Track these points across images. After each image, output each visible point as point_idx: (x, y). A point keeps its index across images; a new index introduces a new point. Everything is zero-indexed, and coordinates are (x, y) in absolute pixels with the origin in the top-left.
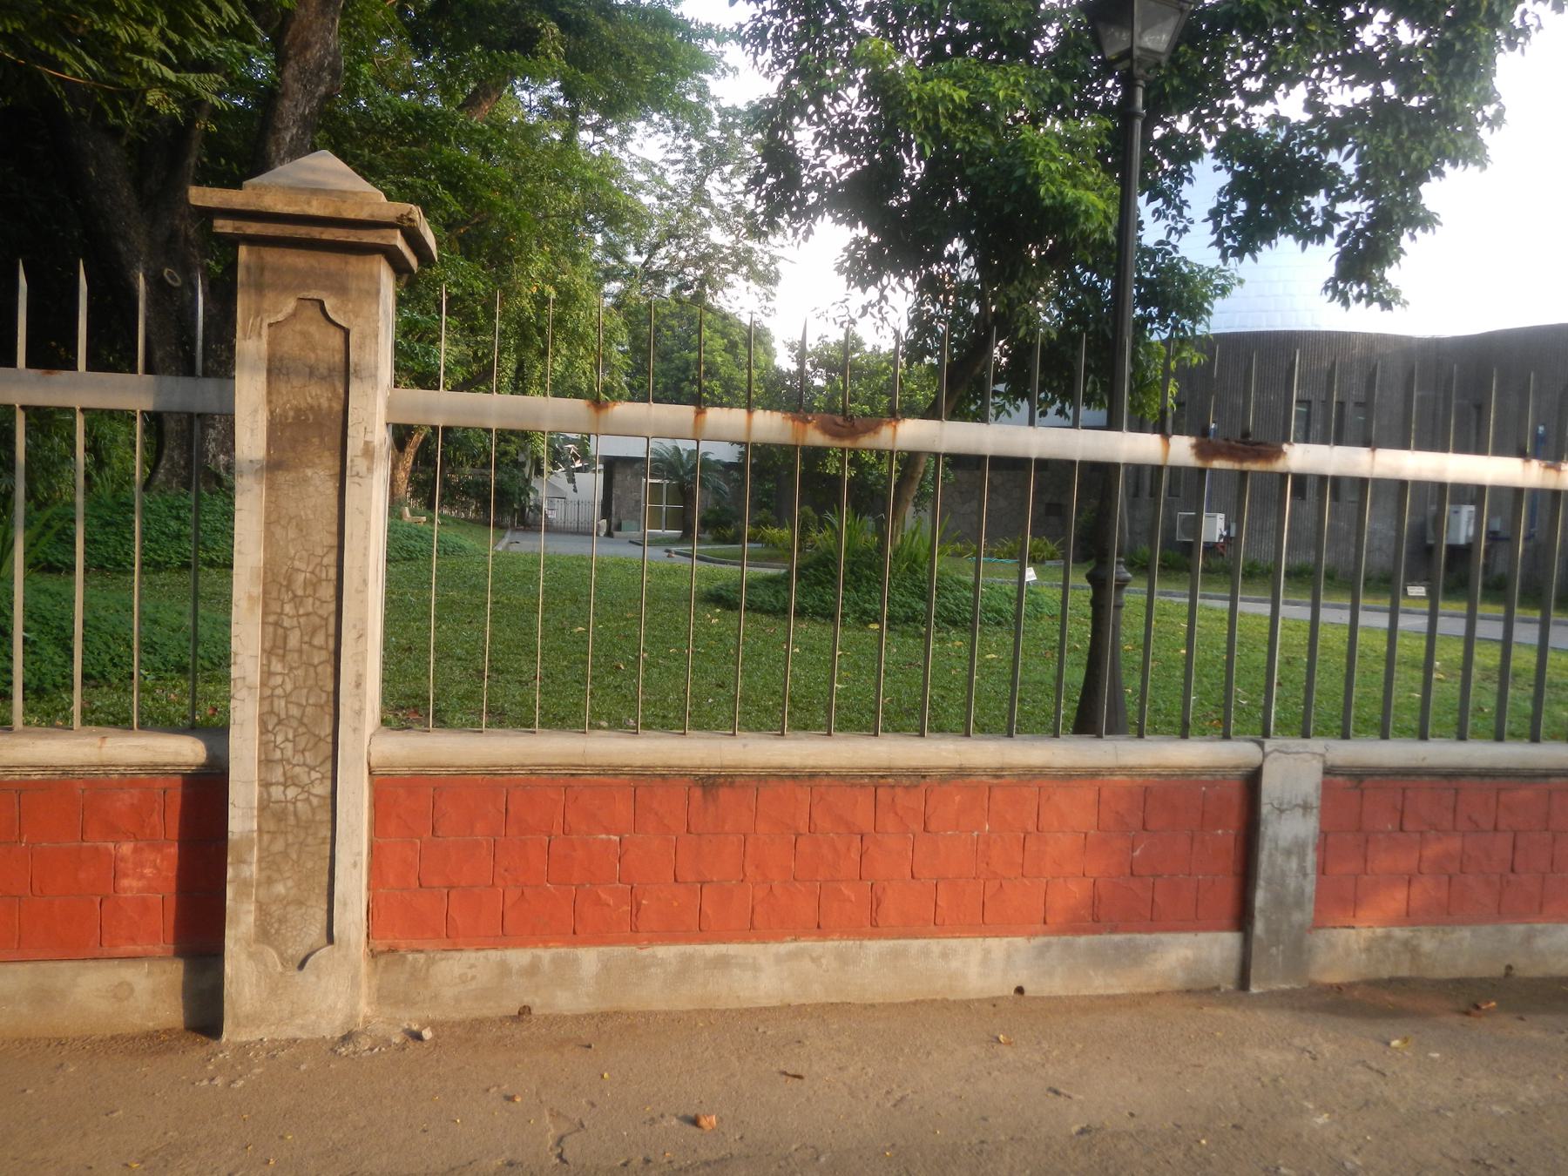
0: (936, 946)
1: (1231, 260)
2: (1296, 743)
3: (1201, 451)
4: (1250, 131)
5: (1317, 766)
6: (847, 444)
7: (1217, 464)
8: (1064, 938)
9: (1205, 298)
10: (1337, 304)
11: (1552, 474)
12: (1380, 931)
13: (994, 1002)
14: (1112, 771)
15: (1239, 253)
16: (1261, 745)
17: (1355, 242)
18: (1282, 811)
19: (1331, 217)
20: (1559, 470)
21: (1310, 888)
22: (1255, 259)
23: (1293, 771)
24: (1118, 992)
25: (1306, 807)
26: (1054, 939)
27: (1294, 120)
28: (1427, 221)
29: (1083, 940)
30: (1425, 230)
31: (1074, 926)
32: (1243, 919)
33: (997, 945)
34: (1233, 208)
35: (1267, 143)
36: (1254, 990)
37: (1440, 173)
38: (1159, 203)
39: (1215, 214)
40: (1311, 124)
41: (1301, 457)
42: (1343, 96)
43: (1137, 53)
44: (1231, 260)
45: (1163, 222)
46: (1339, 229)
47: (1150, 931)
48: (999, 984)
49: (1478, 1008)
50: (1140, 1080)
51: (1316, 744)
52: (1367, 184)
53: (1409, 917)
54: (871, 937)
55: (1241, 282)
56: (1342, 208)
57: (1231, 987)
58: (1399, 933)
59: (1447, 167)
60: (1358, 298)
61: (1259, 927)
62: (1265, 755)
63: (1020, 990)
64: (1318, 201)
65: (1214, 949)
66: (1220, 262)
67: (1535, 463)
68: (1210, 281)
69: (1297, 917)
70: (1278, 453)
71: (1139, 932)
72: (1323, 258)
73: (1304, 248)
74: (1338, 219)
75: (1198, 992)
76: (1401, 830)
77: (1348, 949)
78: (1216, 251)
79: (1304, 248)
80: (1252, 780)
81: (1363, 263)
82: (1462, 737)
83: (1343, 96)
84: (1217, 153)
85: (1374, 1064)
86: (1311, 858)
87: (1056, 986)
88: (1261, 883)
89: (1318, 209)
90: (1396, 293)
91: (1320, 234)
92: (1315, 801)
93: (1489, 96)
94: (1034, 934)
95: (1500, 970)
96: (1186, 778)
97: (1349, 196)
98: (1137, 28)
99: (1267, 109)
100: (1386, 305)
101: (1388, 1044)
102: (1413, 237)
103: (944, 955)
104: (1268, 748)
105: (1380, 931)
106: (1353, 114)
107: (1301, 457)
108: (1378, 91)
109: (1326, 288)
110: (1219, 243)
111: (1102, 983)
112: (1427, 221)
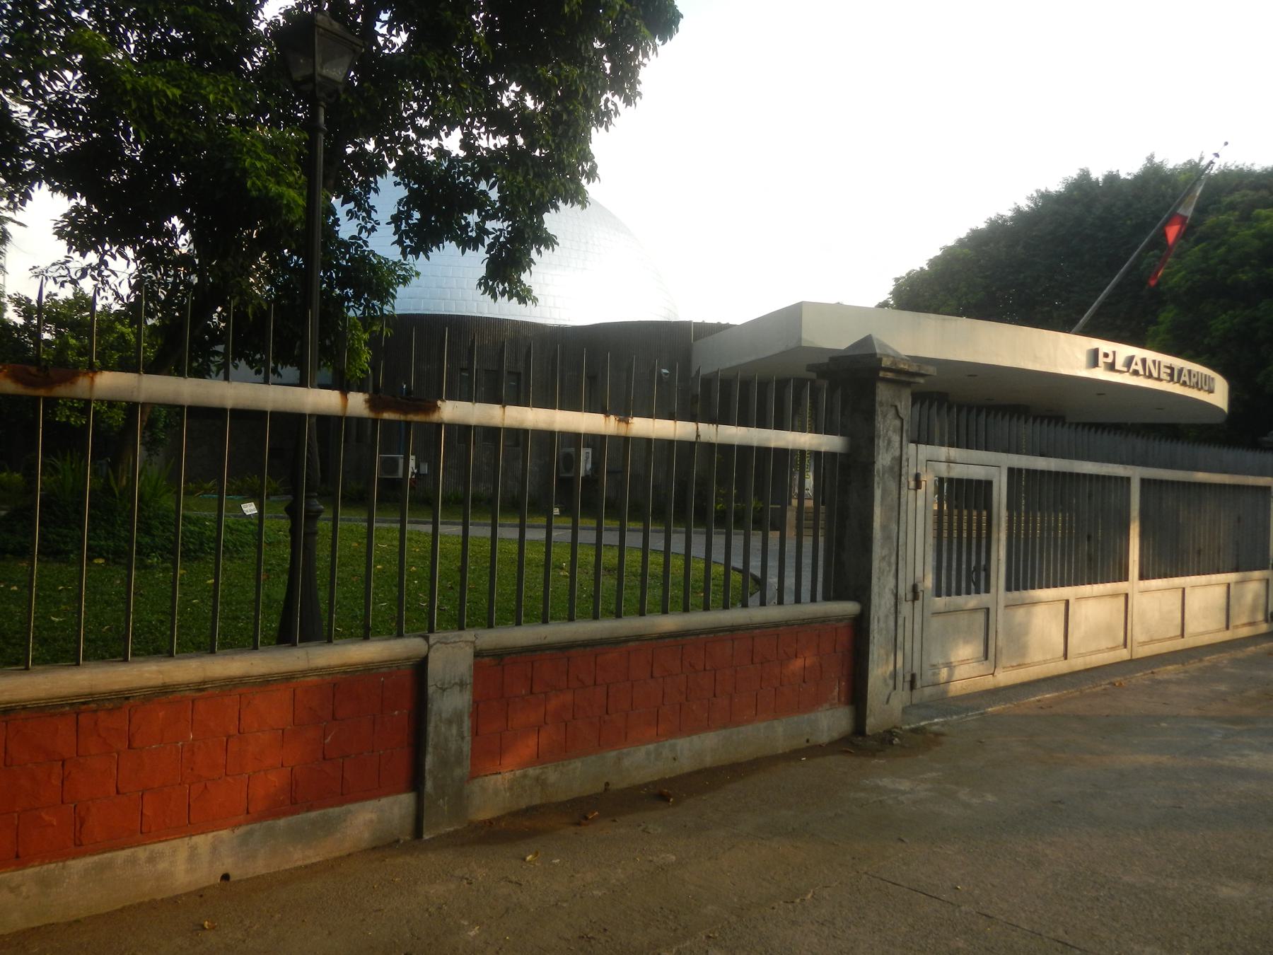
0: (142, 853)
1: (409, 256)
2: (453, 635)
3: (373, 404)
4: (421, 157)
5: (469, 651)
6: (42, 392)
7: (387, 416)
8: (265, 823)
9: (391, 285)
10: (488, 297)
11: (623, 425)
12: (518, 773)
13: (200, 894)
14: (304, 673)
15: (415, 252)
16: (427, 639)
17: (500, 251)
18: (444, 690)
19: (482, 231)
20: (627, 423)
21: (467, 748)
22: (428, 258)
23: (451, 656)
24: (314, 861)
25: (462, 684)
26: (256, 826)
27: (454, 155)
28: (548, 241)
29: (282, 822)
30: (547, 247)
31: (273, 811)
32: (415, 783)
33: (202, 841)
34: (410, 217)
35: (435, 169)
36: (426, 837)
37: (557, 208)
38: (351, 205)
39: (396, 219)
40: (465, 159)
41: (451, 411)
42: (489, 142)
43: (318, 79)
44: (409, 256)
45: (355, 221)
46: (487, 241)
47: (340, 804)
48: (206, 875)
49: (586, 818)
50: (330, 933)
51: (468, 635)
52: (506, 209)
53: (539, 759)
54: (75, 856)
55: (418, 274)
56: (490, 225)
57: (408, 838)
58: (532, 772)
59: (560, 203)
60: (503, 294)
61: (429, 785)
62: (430, 647)
63: (226, 877)
64: (473, 218)
65: (395, 808)
66: (401, 257)
67: (612, 417)
68: (394, 272)
69: (458, 772)
70: (435, 408)
71: (332, 806)
72: (476, 262)
73: (463, 252)
74: (488, 233)
75: (384, 846)
76: (531, 693)
77: (496, 791)
78: (398, 249)
79: (463, 252)
80: (421, 666)
81: (506, 270)
82: (571, 619)
83: (489, 142)
84: (397, 172)
85: (514, 878)
86: (467, 723)
87: (259, 866)
88: (430, 749)
89: (472, 224)
90: (529, 291)
91: (474, 243)
92: (469, 680)
93: (586, 156)
94: (239, 825)
95: (601, 787)
96: (367, 671)
97: (494, 217)
98: (318, 59)
99: (434, 143)
100: (522, 300)
101: (524, 859)
102: (539, 252)
103: (151, 860)
104: (432, 641)
105: (518, 773)
106: (496, 155)
107: (451, 411)
108: (512, 141)
109: (480, 284)
110: (400, 242)
111: (300, 856)
112: (548, 241)
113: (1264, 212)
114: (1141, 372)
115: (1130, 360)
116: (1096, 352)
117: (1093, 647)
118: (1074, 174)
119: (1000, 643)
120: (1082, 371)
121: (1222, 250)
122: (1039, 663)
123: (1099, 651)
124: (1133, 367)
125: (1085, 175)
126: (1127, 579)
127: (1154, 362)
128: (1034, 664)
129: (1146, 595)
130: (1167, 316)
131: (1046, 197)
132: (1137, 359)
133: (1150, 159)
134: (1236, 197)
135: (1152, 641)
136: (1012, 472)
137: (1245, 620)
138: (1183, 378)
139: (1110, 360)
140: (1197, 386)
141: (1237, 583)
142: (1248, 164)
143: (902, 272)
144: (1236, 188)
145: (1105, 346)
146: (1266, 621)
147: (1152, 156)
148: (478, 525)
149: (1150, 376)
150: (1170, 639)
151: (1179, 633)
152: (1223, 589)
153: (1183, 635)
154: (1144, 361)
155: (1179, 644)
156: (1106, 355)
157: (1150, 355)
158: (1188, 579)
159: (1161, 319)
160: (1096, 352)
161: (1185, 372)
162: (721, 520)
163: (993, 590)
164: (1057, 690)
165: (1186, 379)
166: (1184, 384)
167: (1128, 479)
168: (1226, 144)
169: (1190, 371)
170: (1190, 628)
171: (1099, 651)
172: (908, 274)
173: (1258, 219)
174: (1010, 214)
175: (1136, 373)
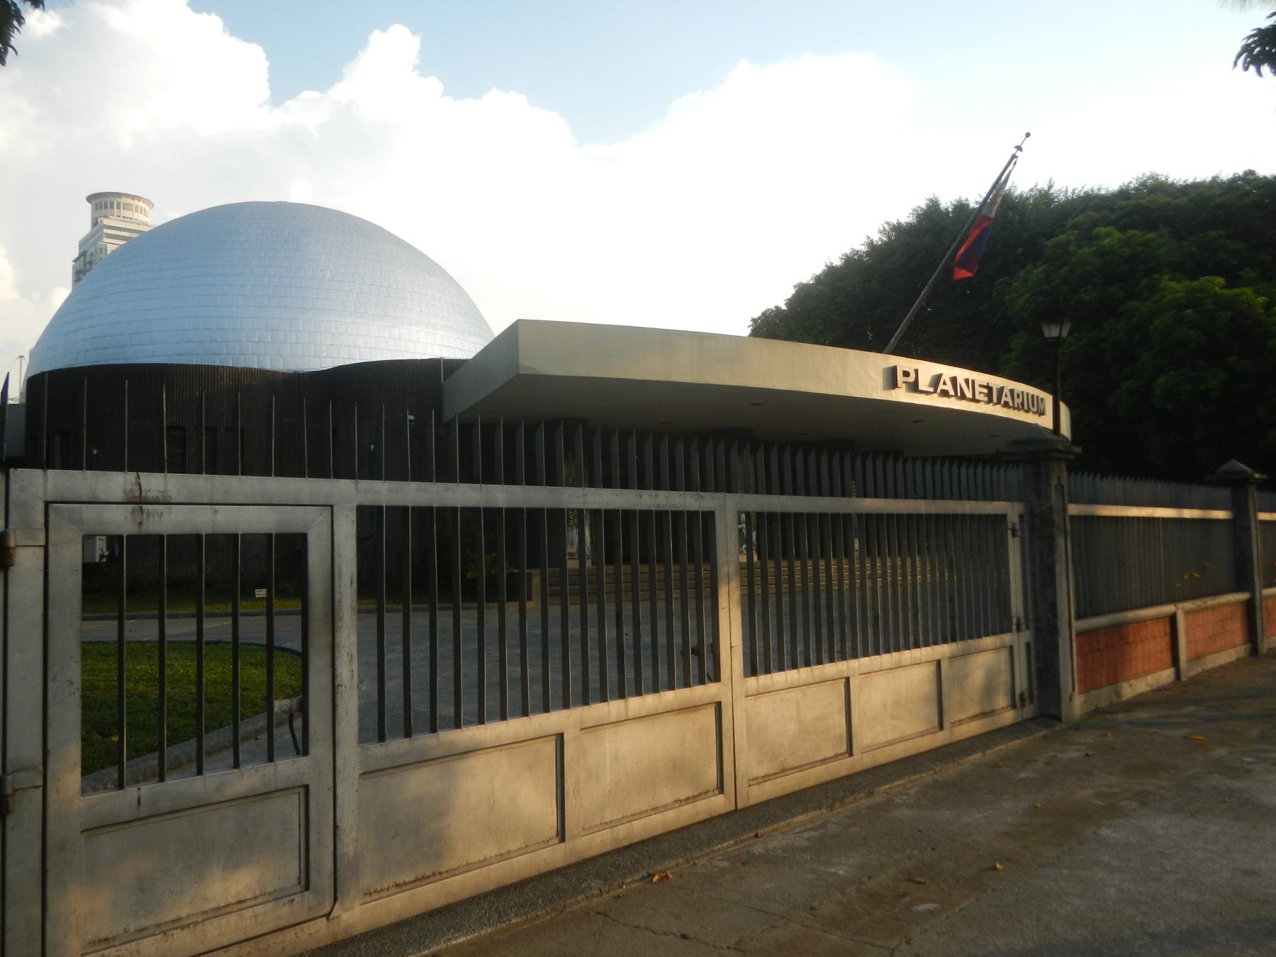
114: (952, 392)
115: (936, 380)
116: (893, 370)
117: (640, 805)
118: (923, 204)
119: (349, 845)
120: (878, 392)
121: (1065, 269)
122: (469, 867)
123: (656, 810)
124: (941, 387)
125: (934, 206)
126: (716, 678)
127: (967, 381)
128: (453, 872)
129: (765, 699)
130: (1018, 342)
131: (898, 229)
132: (946, 378)
134: (1081, 218)
135: (784, 771)
136: (368, 516)
137: (974, 710)
138: (1004, 399)
139: (911, 379)
140: (1021, 407)
141: (952, 658)
142: (1096, 188)
143: (757, 314)
144: (1082, 211)
145: (903, 363)
146: (1013, 706)
148: (134, 618)
149: (963, 397)
150: (824, 761)
151: (844, 748)
152: (929, 670)
153: (850, 752)
154: (954, 380)
155: (843, 767)
156: (906, 374)
157: (962, 374)
159: (1012, 346)
160: (894, 369)
161: (1006, 391)
162: (471, 592)
163: (319, 746)
164: (467, 934)
165: (1009, 399)
166: (1006, 405)
167: (709, 516)
168: (1028, 135)
169: (1012, 391)
171: (656, 810)
172: (764, 314)
173: (1098, 238)
174: (864, 249)
175: (945, 394)
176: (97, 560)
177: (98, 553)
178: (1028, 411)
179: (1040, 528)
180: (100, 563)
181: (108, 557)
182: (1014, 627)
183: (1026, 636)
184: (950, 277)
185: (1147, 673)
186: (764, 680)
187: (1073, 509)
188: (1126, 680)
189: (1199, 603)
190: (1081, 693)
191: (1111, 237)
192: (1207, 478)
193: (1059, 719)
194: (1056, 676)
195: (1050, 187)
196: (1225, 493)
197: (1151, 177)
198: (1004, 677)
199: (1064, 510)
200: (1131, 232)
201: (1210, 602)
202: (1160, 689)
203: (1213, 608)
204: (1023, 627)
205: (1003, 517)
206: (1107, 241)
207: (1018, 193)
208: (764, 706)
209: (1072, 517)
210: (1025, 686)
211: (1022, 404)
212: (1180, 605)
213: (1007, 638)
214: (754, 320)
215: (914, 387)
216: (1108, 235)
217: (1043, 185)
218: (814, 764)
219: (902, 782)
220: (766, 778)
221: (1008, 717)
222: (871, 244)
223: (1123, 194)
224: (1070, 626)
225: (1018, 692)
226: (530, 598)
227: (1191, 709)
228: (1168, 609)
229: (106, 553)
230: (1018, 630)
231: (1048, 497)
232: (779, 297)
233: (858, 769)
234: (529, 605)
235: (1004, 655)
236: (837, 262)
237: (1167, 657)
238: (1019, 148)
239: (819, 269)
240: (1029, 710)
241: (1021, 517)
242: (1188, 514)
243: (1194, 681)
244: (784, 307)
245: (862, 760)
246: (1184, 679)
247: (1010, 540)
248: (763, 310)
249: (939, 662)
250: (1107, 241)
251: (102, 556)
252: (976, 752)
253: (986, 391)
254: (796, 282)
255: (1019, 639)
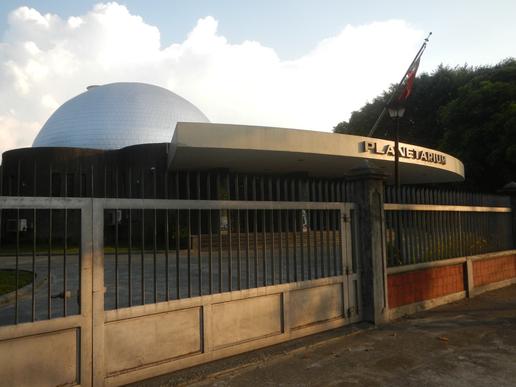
113: (484, 82)
115: (386, 148)
124: (388, 151)
127: (402, 148)
133: (441, 67)
138: (422, 156)
140: (432, 161)
141: (292, 291)
145: (368, 140)
146: (343, 316)
147: (441, 65)
151: (198, 348)
155: (197, 359)
156: (370, 145)
158: (207, 299)
165: (425, 157)
166: (424, 159)
167: (76, 213)
168: (431, 33)
170: (209, 344)
172: (339, 125)
176: (22, 230)
177: (22, 227)
178: (436, 162)
179: (363, 220)
180: (23, 231)
181: (27, 229)
182: (344, 272)
183: (353, 277)
184: (422, 106)
185: (444, 294)
186: (123, 312)
187: (387, 207)
188: (428, 298)
189: (483, 256)
190: (391, 307)
191: (487, 85)
192: (499, 191)
193: (373, 323)
194: (372, 299)
195: (466, 66)
196: (507, 199)
197: (510, 60)
198: (337, 299)
199: (380, 207)
200: (497, 83)
201: (491, 255)
202: (456, 302)
203: (494, 258)
204: (351, 272)
205: (338, 211)
206: (485, 87)
207: (450, 69)
208: (124, 327)
209: (387, 212)
210: (352, 304)
211: (433, 159)
212: (469, 257)
213: (339, 278)
214: (334, 128)
215: (374, 151)
216: (486, 84)
217: (462, 65)
218: (170, 360)
219: (233, 369)
220: (123, 372)
221: (338, 323)
222: (385, 94)
223: (497, 67)
224: (382, 272)
225: (346, 307)
226: (192, 248)
227: (460, 316)
228: (463, 259)
229: (26, 227)
230: (347, 273)
231: (368, 200)
232: (347, 118)
233: (208, 361)
234: (192, 251)
235: (337, 288)
236: (371, 102)
237: (461, 285)
238: (427, 40)
239: (364, 105)
240: (354, 318)
241: (352, 211)
242: (479, 209)
243: (477, 298)
244: (348, 122)
245: (211, 354)
246: (471, 296)
247: (343, 224)
248: (338, 123)
249: (282, 294)
250: (485, 87)
251: (24, 228)
252: (302, 346)
253: (412, 153)
254: (353, 110)
255: (350, 280)
